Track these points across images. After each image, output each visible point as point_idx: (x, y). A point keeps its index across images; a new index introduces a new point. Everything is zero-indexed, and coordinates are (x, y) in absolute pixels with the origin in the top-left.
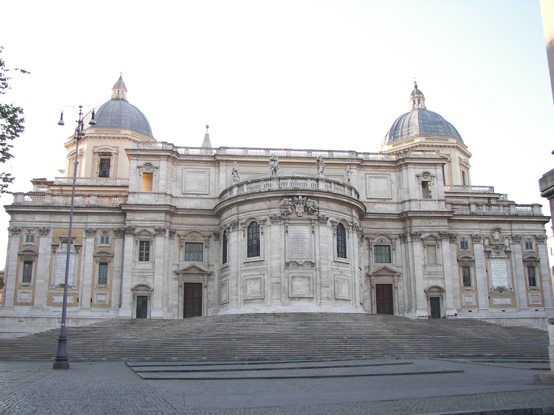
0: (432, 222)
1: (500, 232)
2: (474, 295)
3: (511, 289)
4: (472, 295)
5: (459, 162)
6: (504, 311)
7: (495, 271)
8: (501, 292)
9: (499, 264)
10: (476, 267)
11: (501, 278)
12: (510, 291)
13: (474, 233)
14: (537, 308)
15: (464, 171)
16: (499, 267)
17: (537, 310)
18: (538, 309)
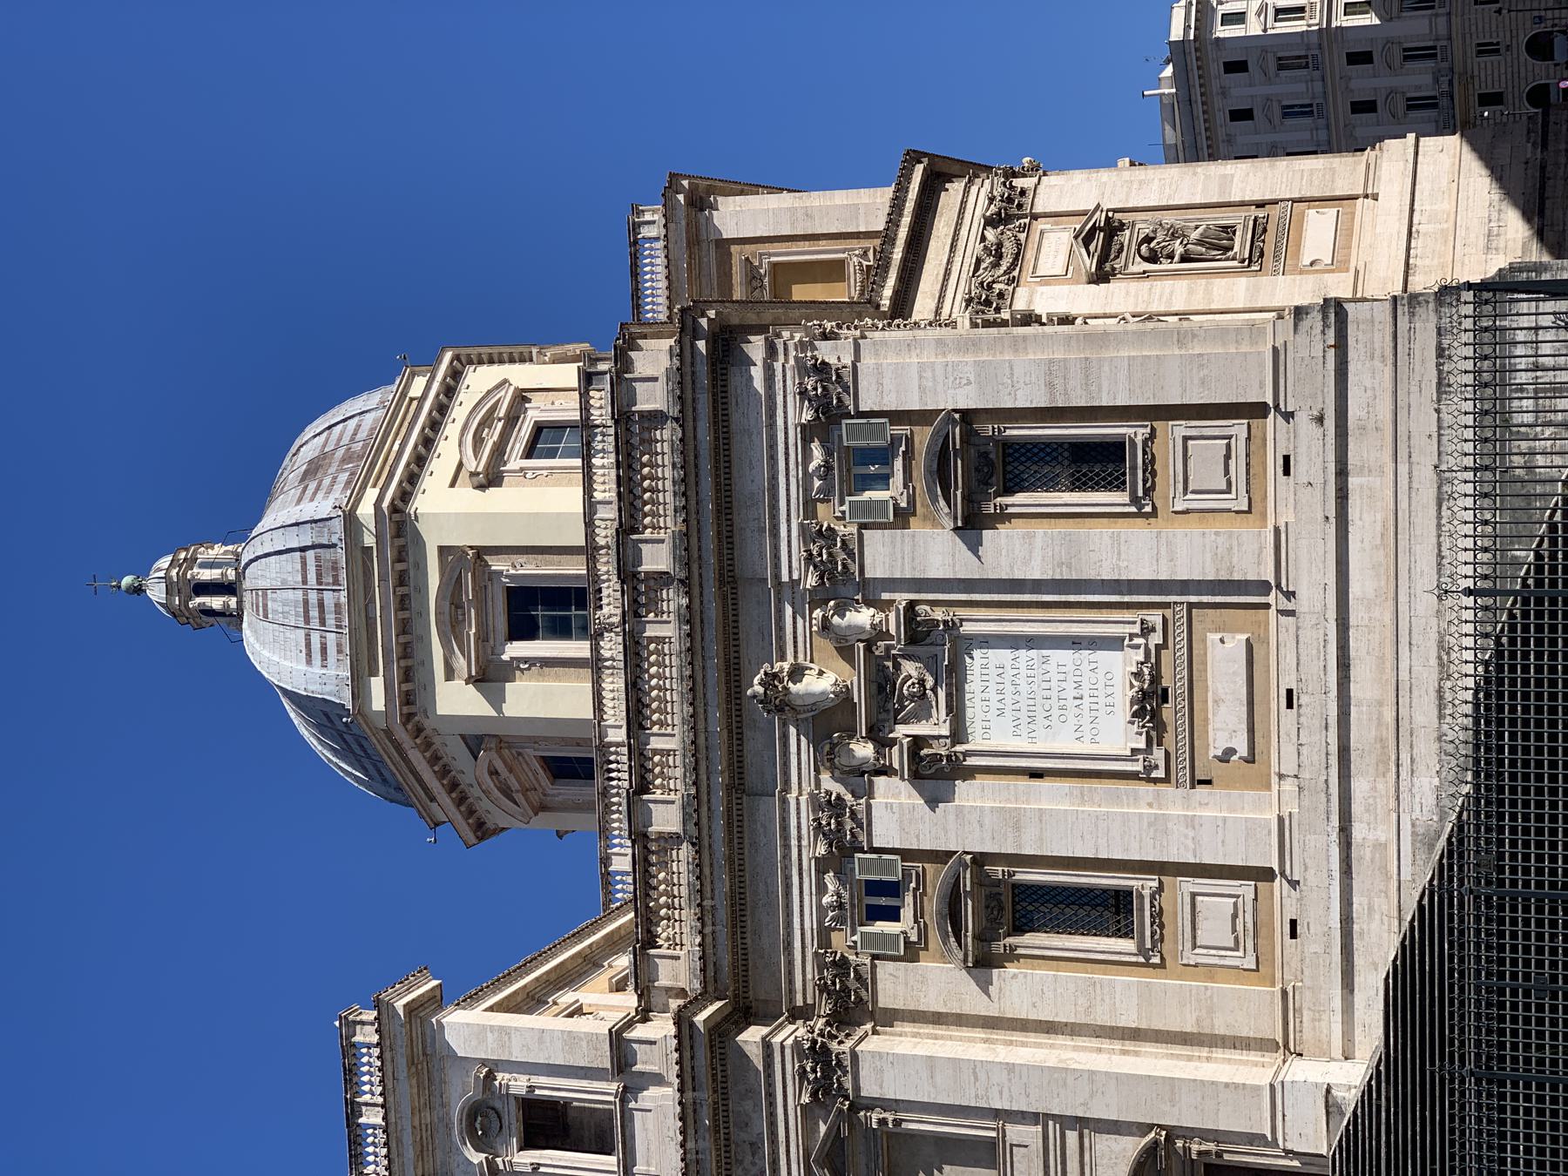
0: (744, 1136)
1: (797, 673)
2: (1188, 885)
3: (1146, 630)
4: (1187, 899)
5: (481, 487)
6: (1290, 692)
7: (1031, 722)
8: (1164, 697)
9: (993, 687)
10: (1009, 849)
11: (1079, 686)
12: (1156, 638)
13: (804, 831)
14: (1273, 465)
15: (525, 431)
16: (1009, 689)
17: (1287, 459)
18: (1281, 452)
